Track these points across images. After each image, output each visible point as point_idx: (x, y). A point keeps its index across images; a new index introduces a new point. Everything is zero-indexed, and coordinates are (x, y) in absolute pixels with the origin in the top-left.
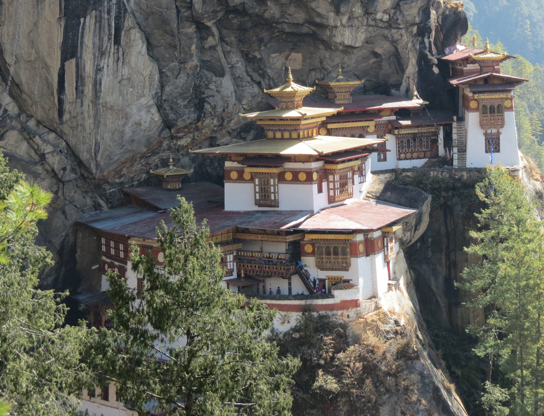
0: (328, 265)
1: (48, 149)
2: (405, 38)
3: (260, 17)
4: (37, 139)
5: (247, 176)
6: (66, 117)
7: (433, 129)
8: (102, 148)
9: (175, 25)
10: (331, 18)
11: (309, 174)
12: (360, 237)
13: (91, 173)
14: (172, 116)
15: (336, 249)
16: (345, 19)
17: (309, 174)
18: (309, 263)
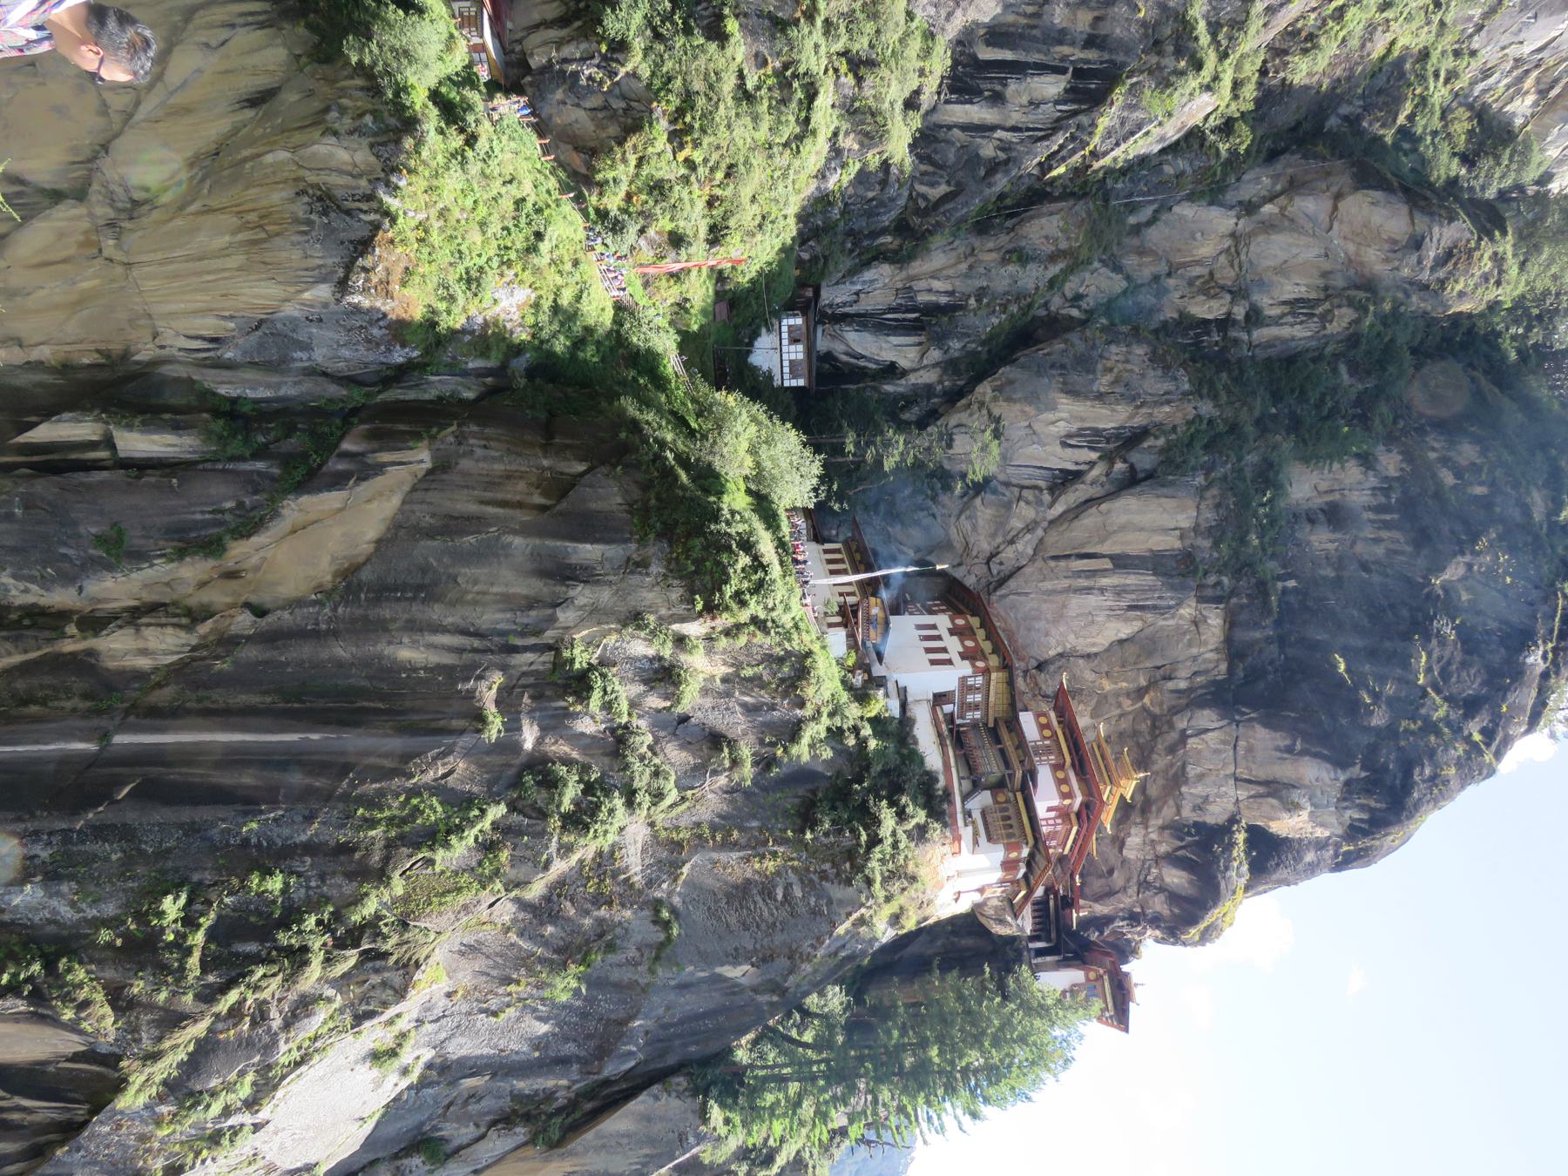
0: (989, 820)
1: (1020, 546)
2: (1128, 900)
3: (1152, 751)
4: (1028, 536)
5: (1047, 733)
6: (1052, 564)
7: (1053, 935)
8: (1023, 598)
9: (1148, 664)
10: (1155, 822)
11: (1069, 795)
12: (1025, 852)
13: (995, 590)
14: (1052, 668)
15: (1011, 826)
16: (1154, 836)
17: (1069, 795)
18: (984, 799)
